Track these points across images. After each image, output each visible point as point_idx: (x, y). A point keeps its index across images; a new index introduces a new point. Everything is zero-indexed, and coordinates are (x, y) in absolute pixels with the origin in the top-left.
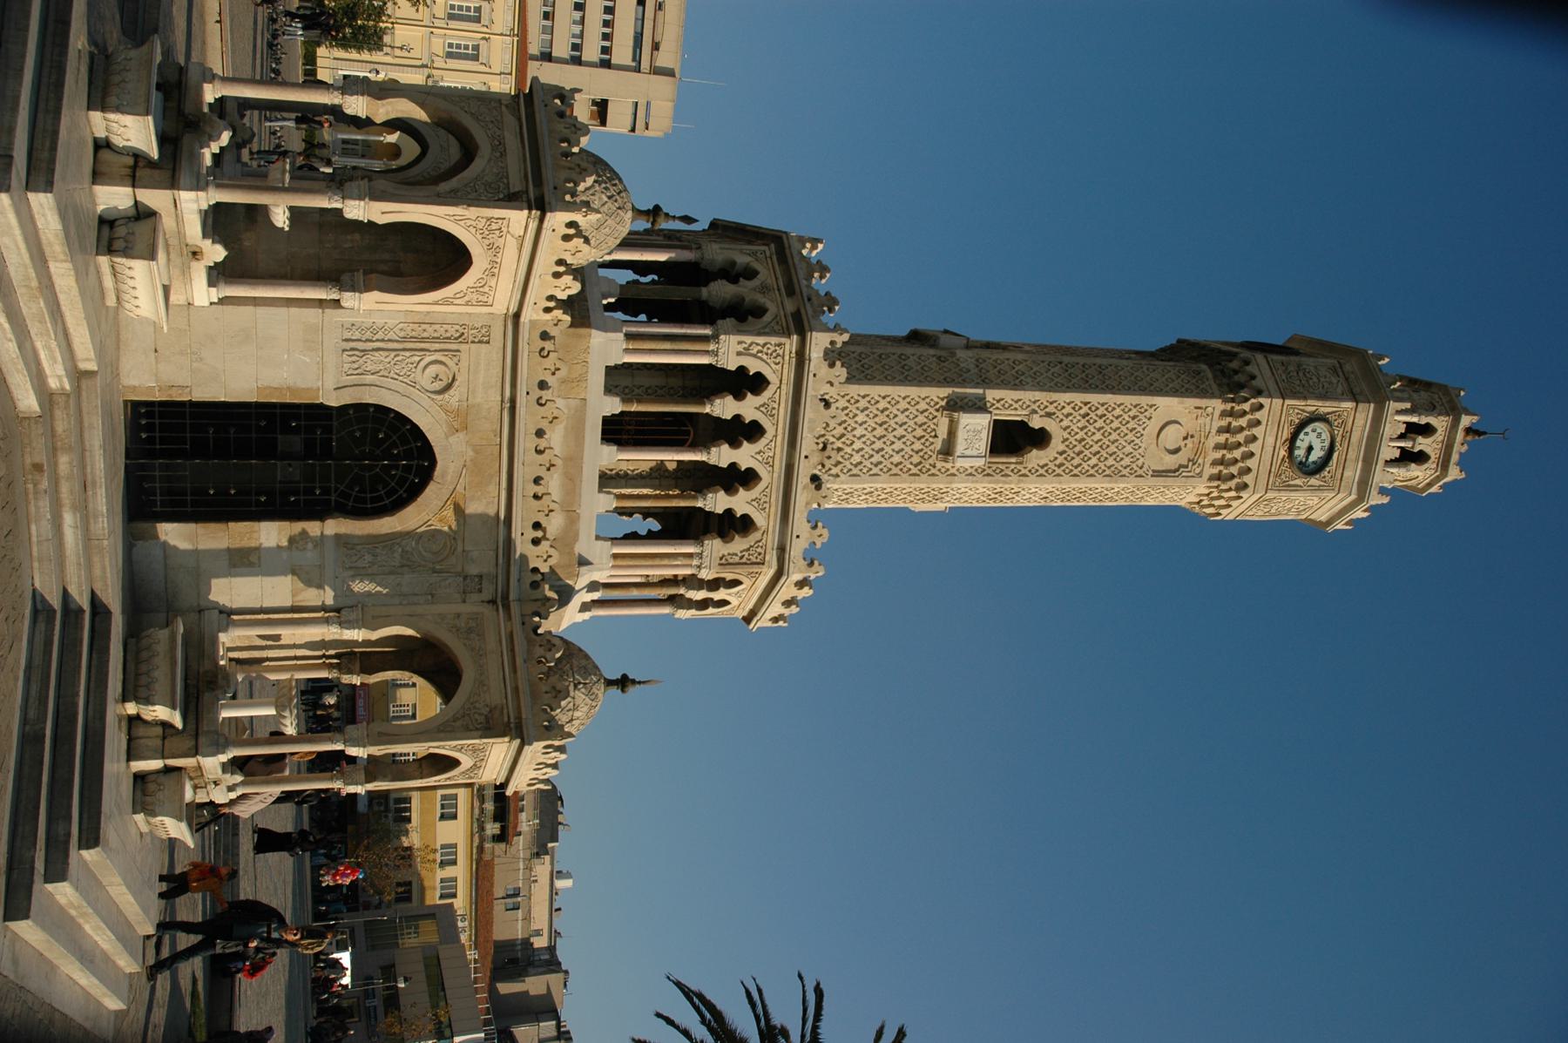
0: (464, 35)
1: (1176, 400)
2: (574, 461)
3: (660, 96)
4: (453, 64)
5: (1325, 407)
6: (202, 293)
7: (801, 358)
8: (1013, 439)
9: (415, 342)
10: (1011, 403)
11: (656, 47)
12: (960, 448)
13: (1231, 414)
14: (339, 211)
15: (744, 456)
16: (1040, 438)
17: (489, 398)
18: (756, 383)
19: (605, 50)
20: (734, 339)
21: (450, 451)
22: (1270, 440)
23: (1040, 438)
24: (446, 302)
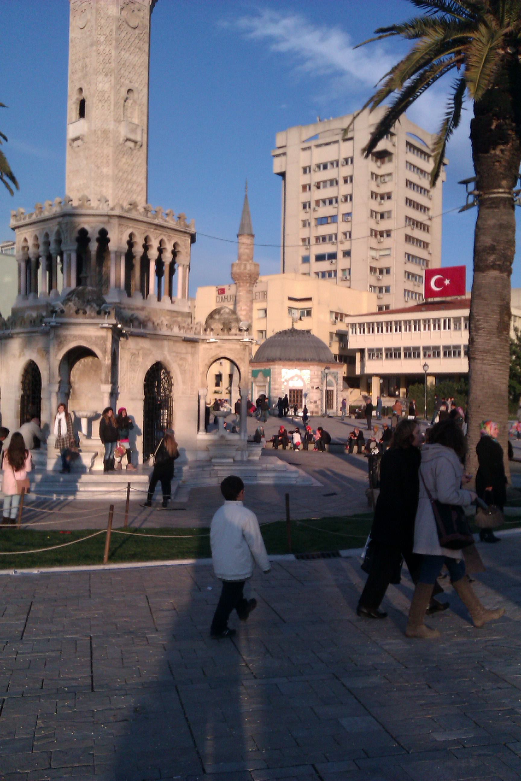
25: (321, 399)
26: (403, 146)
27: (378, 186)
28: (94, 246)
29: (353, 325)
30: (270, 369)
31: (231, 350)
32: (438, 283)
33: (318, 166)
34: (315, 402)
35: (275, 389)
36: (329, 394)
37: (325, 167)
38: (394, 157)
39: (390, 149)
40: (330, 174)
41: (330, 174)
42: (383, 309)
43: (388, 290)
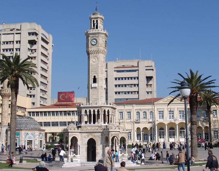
0: (126, 115)
1: (90, 61)
2: (92, 126)
3: (144, 64)
4: (132, 117)
5: (90, 41)
6: (78, 155)
7: (83, 107)
8: (95, 81)
9: (82, 140)
10: (91, 81)
11: (133, 66)
12: (95, 86)
13: (91, 53)
14: (70, 146)
15: (92, 111)
16: (95, 76)
17: (86, 134)
18: (86, 110)
19: (135, 78)
20: (82, 113)
21: (90, 137)
22: (93, 48)
23: (95, 76)
24: (79, 138)
25: (39, 144)
26: (40, 39)
27: (30, 54)
28: (107, 113)
29: (29, 112)
30: (19, 132)
31: (124, 135)
32: (63, 97)
33: (4, 43)
34: (37, 145)
35: (22, 140)
36: (41, 141)
37: (7, 43)
38: (37, 43)
39: (36, 40)
40: (10, 46)
41: (10, 46)
42: (43, 106)
43: (34, 96)
